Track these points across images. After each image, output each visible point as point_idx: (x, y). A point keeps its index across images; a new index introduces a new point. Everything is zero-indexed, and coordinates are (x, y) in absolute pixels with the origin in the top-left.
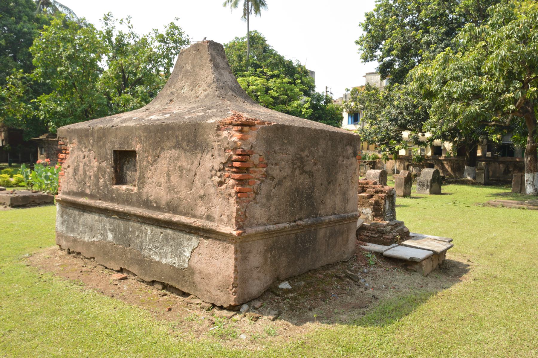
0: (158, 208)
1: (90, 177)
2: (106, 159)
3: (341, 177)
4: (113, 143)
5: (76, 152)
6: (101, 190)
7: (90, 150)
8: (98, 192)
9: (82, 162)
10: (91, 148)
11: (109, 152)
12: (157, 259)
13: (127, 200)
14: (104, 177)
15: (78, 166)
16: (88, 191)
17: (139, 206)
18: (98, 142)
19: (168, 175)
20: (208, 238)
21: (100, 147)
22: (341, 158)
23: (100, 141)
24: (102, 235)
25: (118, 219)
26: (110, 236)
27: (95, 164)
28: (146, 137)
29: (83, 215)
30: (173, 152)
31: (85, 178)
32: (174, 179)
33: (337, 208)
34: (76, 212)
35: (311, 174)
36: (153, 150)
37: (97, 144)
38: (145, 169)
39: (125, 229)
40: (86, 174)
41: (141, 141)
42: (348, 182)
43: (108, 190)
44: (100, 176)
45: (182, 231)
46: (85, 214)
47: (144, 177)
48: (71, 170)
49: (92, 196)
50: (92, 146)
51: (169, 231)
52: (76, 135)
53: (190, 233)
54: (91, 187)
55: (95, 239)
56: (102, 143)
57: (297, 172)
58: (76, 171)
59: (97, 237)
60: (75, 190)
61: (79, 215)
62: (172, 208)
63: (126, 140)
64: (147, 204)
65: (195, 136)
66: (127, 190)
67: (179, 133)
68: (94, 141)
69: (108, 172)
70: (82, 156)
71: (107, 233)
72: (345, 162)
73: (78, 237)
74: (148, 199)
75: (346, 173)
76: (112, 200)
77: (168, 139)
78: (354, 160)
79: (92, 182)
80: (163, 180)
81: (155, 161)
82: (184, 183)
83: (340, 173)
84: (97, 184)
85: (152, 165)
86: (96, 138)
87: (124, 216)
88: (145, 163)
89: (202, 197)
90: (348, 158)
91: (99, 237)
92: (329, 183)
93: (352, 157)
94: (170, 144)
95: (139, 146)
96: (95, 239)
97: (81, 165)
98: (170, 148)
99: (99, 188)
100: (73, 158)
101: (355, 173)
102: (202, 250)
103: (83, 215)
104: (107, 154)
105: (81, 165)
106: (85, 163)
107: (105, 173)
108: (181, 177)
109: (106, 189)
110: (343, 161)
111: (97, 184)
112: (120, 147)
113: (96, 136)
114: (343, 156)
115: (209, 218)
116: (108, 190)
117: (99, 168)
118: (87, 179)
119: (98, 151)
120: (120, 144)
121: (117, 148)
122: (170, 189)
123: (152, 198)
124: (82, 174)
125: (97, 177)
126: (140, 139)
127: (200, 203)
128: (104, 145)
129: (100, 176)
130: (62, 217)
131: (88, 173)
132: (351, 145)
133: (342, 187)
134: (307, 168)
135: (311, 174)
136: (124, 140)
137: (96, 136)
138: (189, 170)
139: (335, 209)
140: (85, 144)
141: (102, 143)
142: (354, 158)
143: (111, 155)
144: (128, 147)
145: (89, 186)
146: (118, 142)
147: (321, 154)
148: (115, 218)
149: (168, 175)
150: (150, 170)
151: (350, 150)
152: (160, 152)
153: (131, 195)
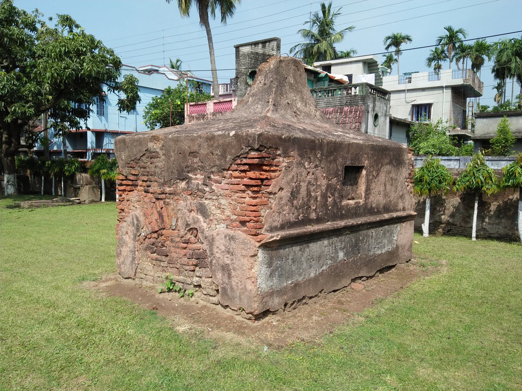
0: (379, 212)
1: (317, 198)
2: (337, 175)
4: (344, 158)
5: (295, 169)
6: (329, 210)
7: (316, 166)
8: (326, 213)
9: (304, 181)
10: (318, 163)
11: (340, 168)
12: (379, 252)
13: (355, 212)
14: (333, 195)
15: (298, 187)
16: (313, 216)
17: (365, 216)
18: (327, 157)
19: (385, 185)
20: (404, 222)
21: (330, 162)
23: (331, 156)
24: (332, 258)
25: (349, 234)
26: (341, 255)
27: (324, 182)
28: (372, 155)
29: (308, 247)
30: (388, 168)
31: (309, 200)
32: (388, 187)
34: (296, 248)
36: (377, 165)
37: (326, 159)
38: (371, 182)
39: (356, 241)
40: (311, 195)
41: (368, 158)
43: (338, 208)
44: (329, 194)
45: (392, 224)
46: (311, 245)
47: (370, 189)
48: (285, 194)
49: (319, 220)
50: (320, 161)
51: (386, 227)
52: (296, 146)
53: (396, 223)
54: (318, 210)
55: (324, 268)
56: (332, 158)
58: (294, 194)
59: (327, 264)
60: (292, 218)
61: (300, 250)
62: (387, 209)
63: (357, 157)
64: (371, 211)
65: (399, 156)
66: (356, 203)
67: (391, 153)
68: (322, 155)
69: (339, 190)
70: (304, 173)
71: (338, 253)
73: (300, 279)
74: (372, 206)
76: (342, 217)
77: (386, 157)
79: (318, 203)
80: (382, 188)
81: (378, 175)
82: (393, 189)
84: (325, 205)
85: (376, 178)
86: (325, 152)
87: (353, 229)
88: (371, 177)
89: (401, 197)
91: (329, 262)
94: (387, 161)
95: (367, 162)
96: (324, 268)
97: (304, 185)
98: (386, 164)
99: (327, 209)
100: (290, 177)
102: (403, 231)
103: (308, 247)
104: (338, 170)
105: (304, 185)
106: (309, 183)
107: (335, 191)
108: (392, 185)
109: (336, 208)
111: (325, 205)
112: (352, 163)
113: (325, 149)
115: (404, 209)
116: (338, 208)
117: (329, 186)
118: (312, 202)
119: (328, 167)
120: (352, 160)
121: (348, 163)
122: (386, 195)
123: (374, 205)
124: (305, 196)
125: (325, 197)
126: (368, 156)
127: (400, 200)
128: (335, 160)
129: (329, 194)
130: (270, 264)
131: (313, 194)
136: (356, 156)
137: (325, 149)
138: (396, 180)
140: (310, 158)
141: (332, 158)
143: (342, 171)
144: (359, 163)
145: (315, 210)
146: (349, 158)
148: (347, 234)
149: (385, 185)
150: (375, 181)
152: (381, 167)
153: (359, 207)
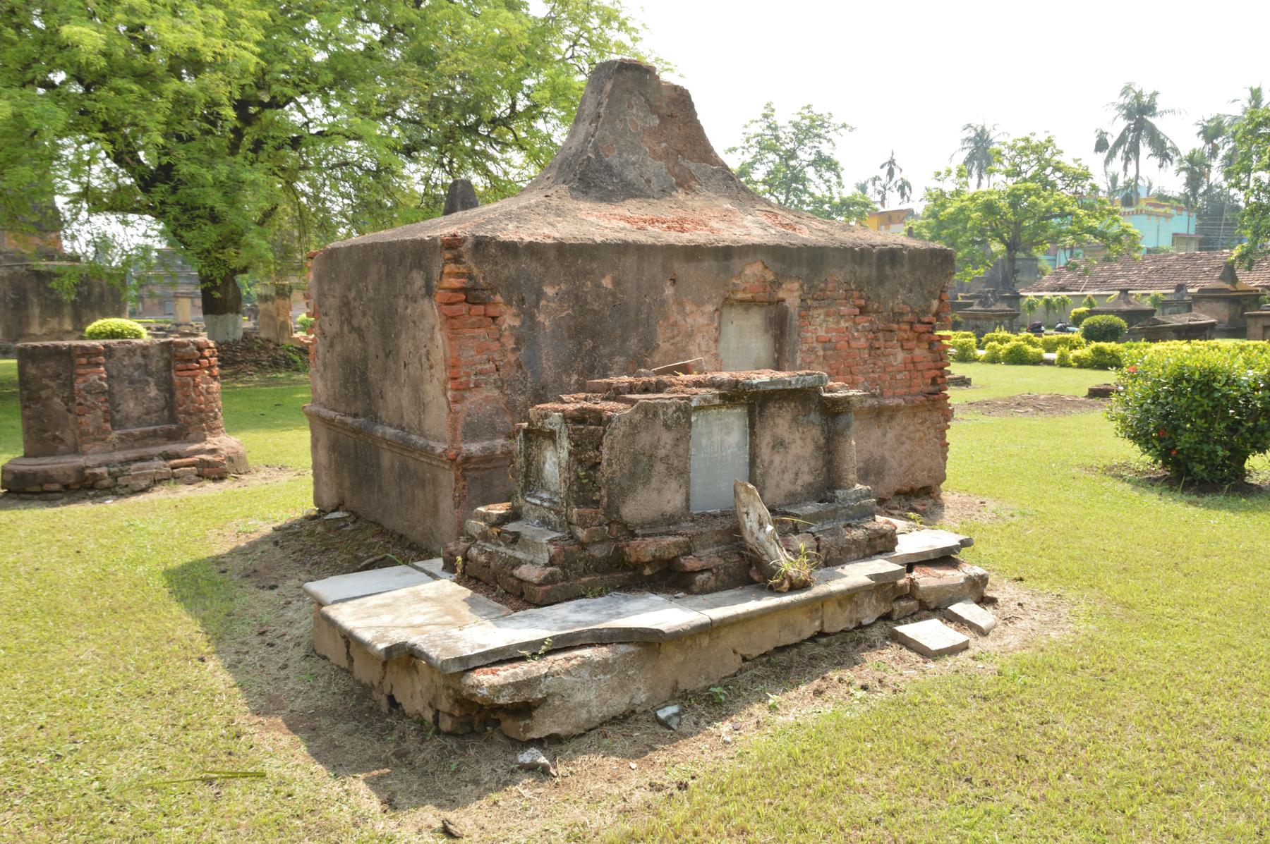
3: (406, 345)
22: (401, 301)
33: (405, 417)
35: (360, 332)
42: (420, 359)
57: (346, 328)
72: (409, 311)
75: (414, 338)
78: (425, 304)
83: (404, 336)
90: (415, 301)
92: (387, 356)
93: (423, 297)
101: (432, 339)
110: (406, 308)
114: (407, 296)
132: (420, 267)
133: (411, 371)
134: (355, 323)
135: (360, 332)
139: (402, 417)
142: (426, 301)
147: (371, 293)
151: (418, 280)
